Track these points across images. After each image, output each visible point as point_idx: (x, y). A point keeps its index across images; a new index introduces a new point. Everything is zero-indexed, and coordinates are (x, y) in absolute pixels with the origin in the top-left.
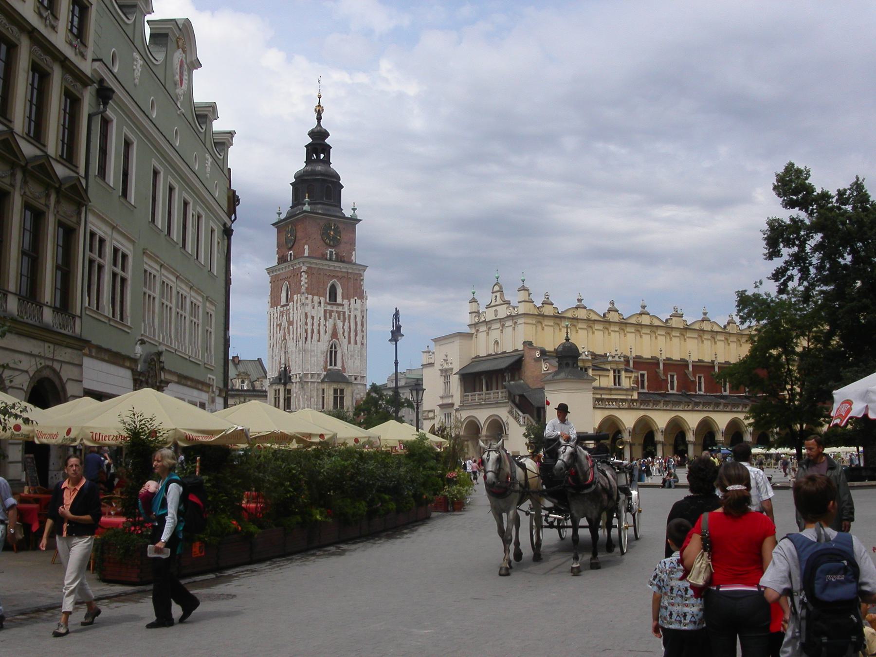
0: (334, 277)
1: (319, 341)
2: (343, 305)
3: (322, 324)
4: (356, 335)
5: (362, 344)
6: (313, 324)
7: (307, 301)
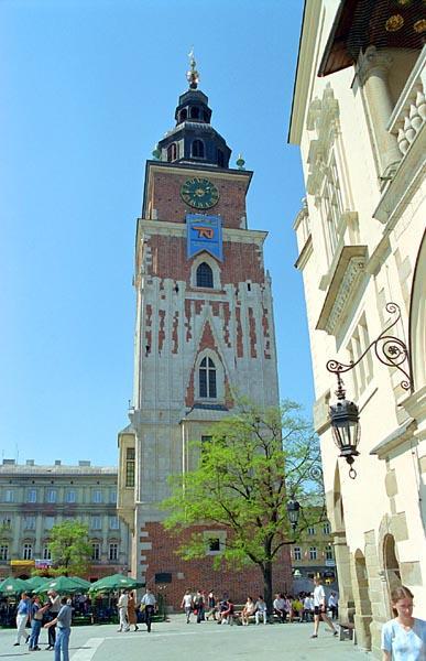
1: (175, 352)
2: (224, 292)
3: (180, 324)
4: (253, 341)
5: (268, 357)
6: (162, 324)
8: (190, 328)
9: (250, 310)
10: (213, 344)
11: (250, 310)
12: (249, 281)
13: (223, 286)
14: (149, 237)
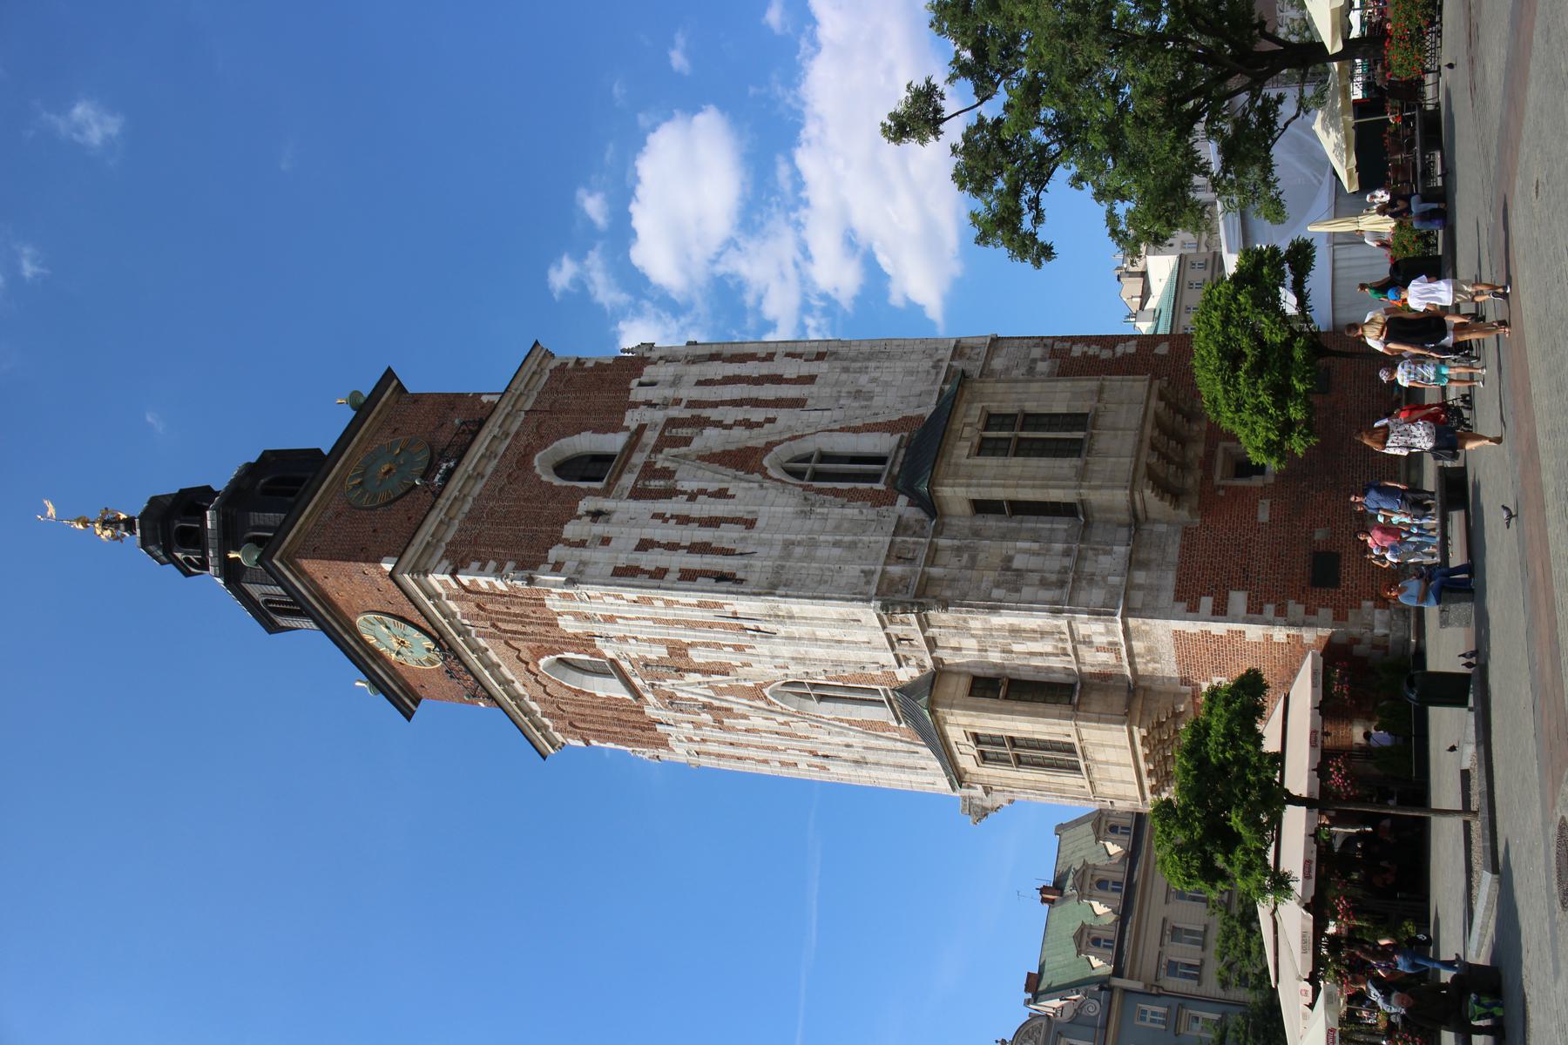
0: (525, 460)
2: (642, 428)
4: (777, 379)
5: (820, 356)
6: (673, 547)
7: (570, 566)
8: (703, 492)
9: (699, 383)
10: (755, 450)
12: (635, 382)
13: (627, 429)
14: (445, 563)
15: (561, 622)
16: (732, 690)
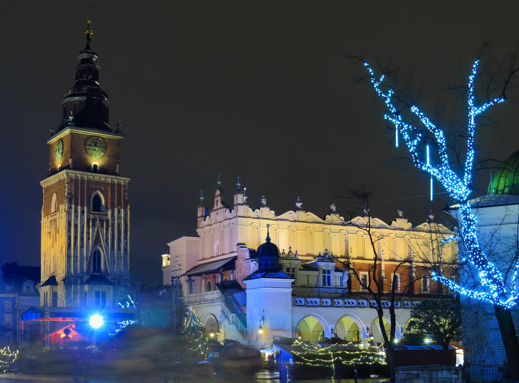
2: (107, 215)
6: (76, 232)
8: (89, 235)
11: (119, 225)
12: (119, 208)
14: (69, 180)
15: (61, 206)
16: (53, 240)
